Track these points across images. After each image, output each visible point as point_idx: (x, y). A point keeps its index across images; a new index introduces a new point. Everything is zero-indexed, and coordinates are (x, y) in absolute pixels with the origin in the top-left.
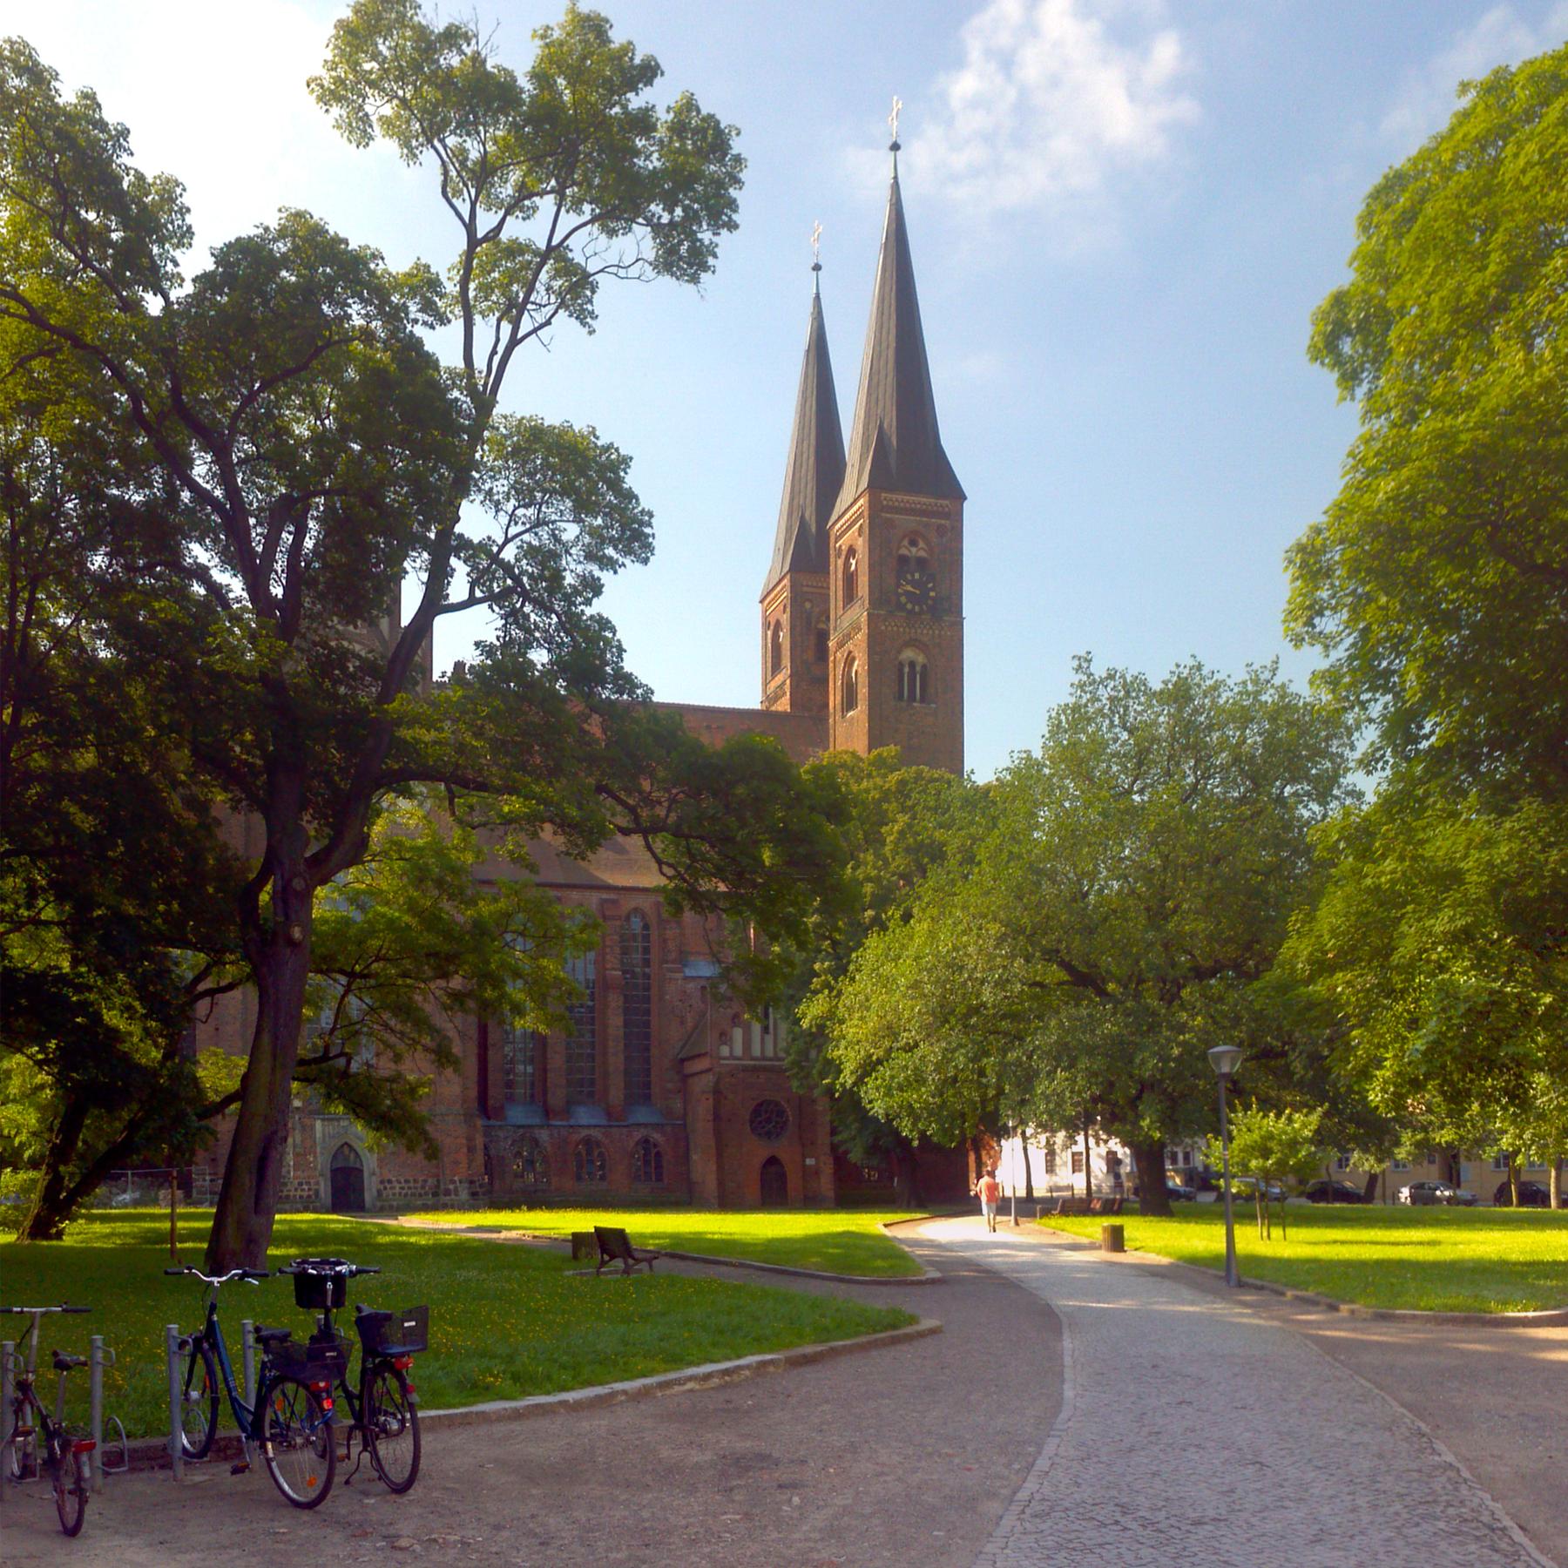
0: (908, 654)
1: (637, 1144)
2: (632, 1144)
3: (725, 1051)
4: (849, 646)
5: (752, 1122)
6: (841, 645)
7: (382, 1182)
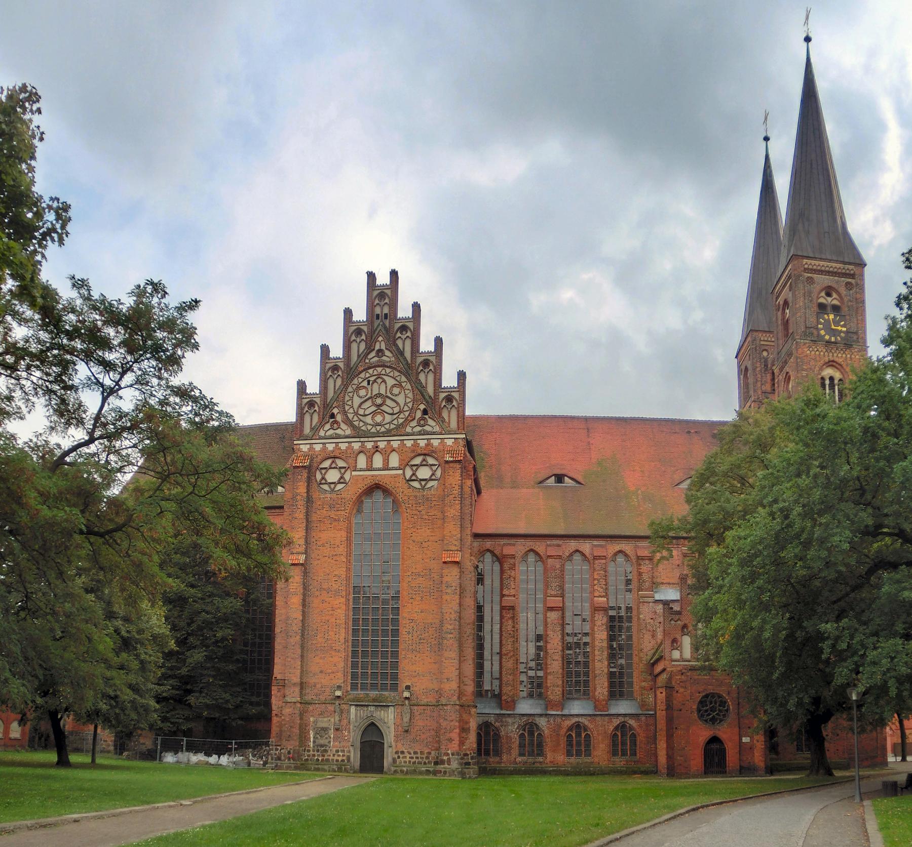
0: (828, 372)
1: (616, 728)
2: (612, 728)
3: (676, 654)
4: (787, 369)
5: (699, 711)
6: (781, 370)
7: (397, 753)
